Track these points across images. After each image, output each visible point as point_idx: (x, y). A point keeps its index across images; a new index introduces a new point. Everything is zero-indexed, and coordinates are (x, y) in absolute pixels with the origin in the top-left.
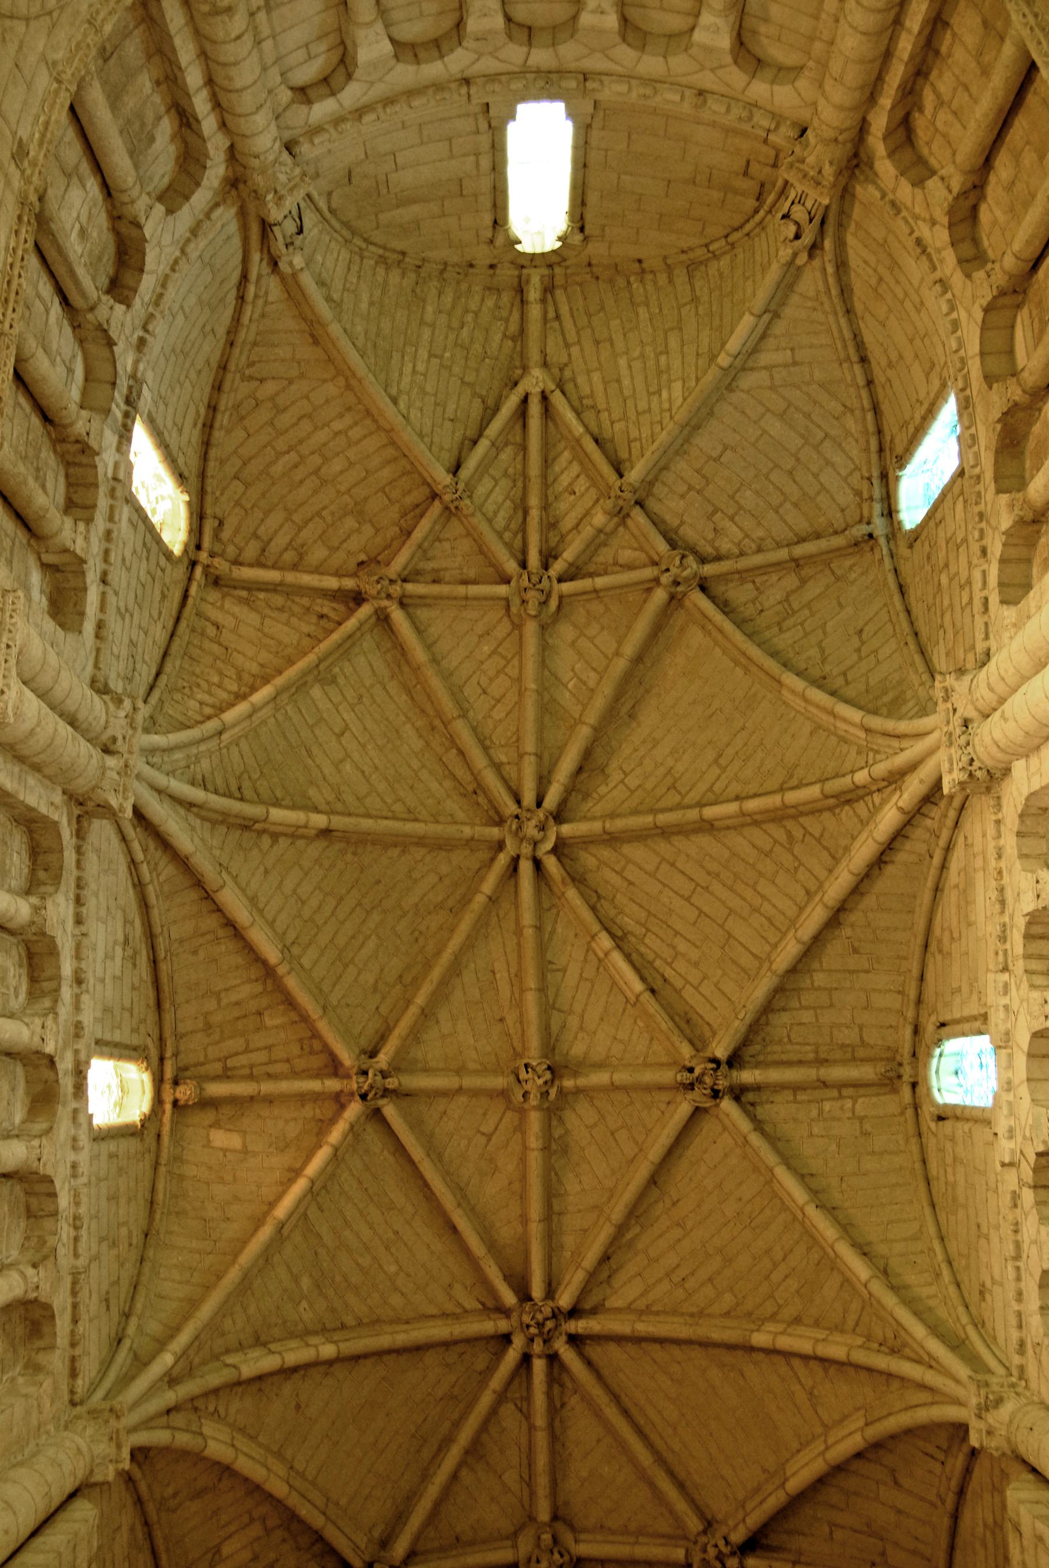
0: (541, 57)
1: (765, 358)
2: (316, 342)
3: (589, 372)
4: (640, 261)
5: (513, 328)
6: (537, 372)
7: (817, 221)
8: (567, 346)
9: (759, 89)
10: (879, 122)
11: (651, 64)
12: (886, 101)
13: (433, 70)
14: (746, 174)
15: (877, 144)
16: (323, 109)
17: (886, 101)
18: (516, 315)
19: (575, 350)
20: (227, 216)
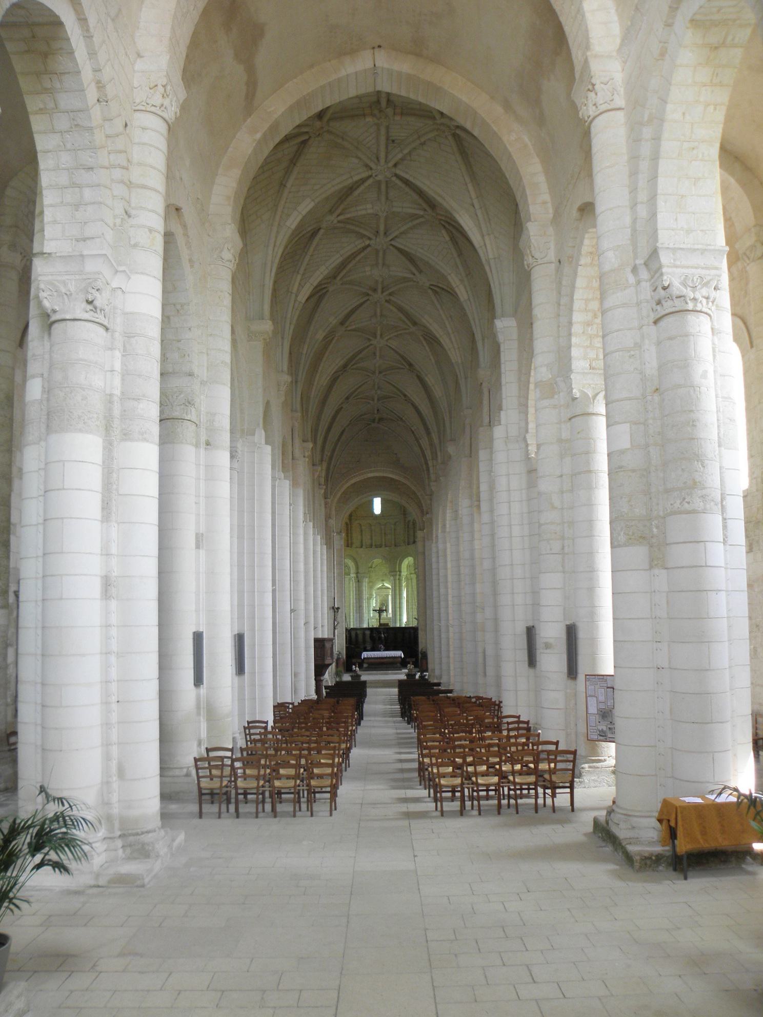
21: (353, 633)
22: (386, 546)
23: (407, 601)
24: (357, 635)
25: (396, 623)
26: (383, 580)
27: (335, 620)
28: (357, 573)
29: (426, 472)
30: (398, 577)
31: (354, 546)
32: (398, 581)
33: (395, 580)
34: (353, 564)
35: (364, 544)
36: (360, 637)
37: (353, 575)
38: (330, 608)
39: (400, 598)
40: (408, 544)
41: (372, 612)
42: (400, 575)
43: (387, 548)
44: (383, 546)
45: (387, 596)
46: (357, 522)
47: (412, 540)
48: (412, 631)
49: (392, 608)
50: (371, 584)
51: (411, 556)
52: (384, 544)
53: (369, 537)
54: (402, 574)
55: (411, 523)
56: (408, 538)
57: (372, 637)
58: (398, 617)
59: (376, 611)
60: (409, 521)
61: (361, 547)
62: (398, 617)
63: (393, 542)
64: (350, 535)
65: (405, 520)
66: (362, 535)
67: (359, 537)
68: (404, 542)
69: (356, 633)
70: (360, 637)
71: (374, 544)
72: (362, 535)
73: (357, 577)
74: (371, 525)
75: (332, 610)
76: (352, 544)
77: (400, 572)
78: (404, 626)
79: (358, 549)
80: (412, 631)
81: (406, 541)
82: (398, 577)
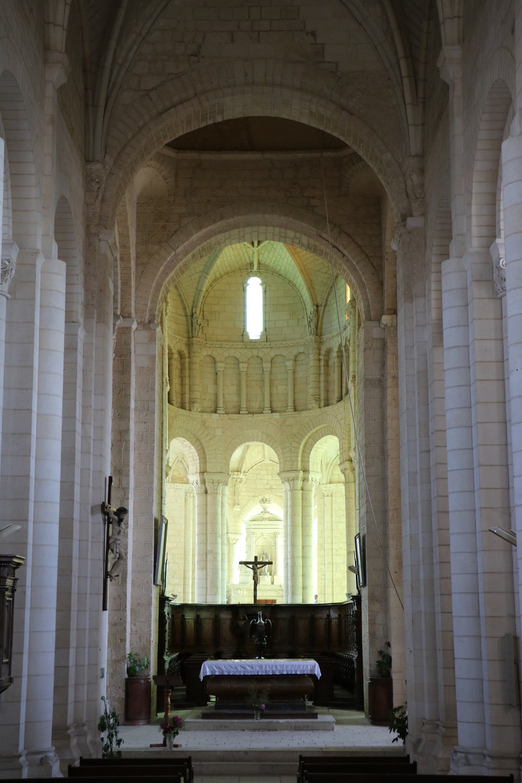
0: (255, 352)
1: (197, 276)
2: (311, 280)
3: (241, 248)
4: (228, 276)
5: (261, 256)
6: (255, 251)
7: (194, 328)
8: (246, 252)
9: (209, 353)
10: (187, 360)
11: (232, 352)
12: (187, 364)
13: (278, 352)
14: (208, 321)
15: (186, 352)
16: (301, 350)
17: (187, 364)
18: (260, 258)
19: (244, 251)
20: (325, 337)
21: (190, 616)
22: (272, 411)
23: (322, 547)
24: (198, 621)
25: (293, 594)
26: (264, 501)
27: (108, 547)
28: (203, 472)
29: (406, 81)
30: (300, 483)
31: (197, 407)
32: (299, 494)
33: (293, 490)
34: (193, 450)
35: (221, 404)
36: (208, 626)
37: (194, 478)
38: (93, 511)
39: (305, 536)
40: (327, 404)
41: (236, 565)
42: (305, 480)
43: (276, 415)
44: (267, 411)
45: (275, 535)
46: (205, 352)
47: (335, 395)
48: (334, 615)
49: (286, 558)
50: (237, 509)
51: (333, 433)
52: (267, 404)
53: (233, 389)
54: (311, 476)
55: (334, 354)
56: (327, 391)
57: (234, 627)
58: (300, 579)
59: (246, 563)
60: (329, 352)
61: (215, 412)
62: (300, 579)
63: (290, 403)
64: (187, 381)
65: (320, 349)
66: (216, 383)
67: (211, 389)
68: (318, 400)
69: (198, 616)
70: (208, 626)
71: (244, 405)
72: (216, 383)
73: (204, 482)
74: (238, 362)
75: (100, 517)
76: (192, 402)
77: (306, 471)
78: (312, 601)
79: (205, 415)
80: (334, 615)
81: (322, 397)
82: (300, 483)
